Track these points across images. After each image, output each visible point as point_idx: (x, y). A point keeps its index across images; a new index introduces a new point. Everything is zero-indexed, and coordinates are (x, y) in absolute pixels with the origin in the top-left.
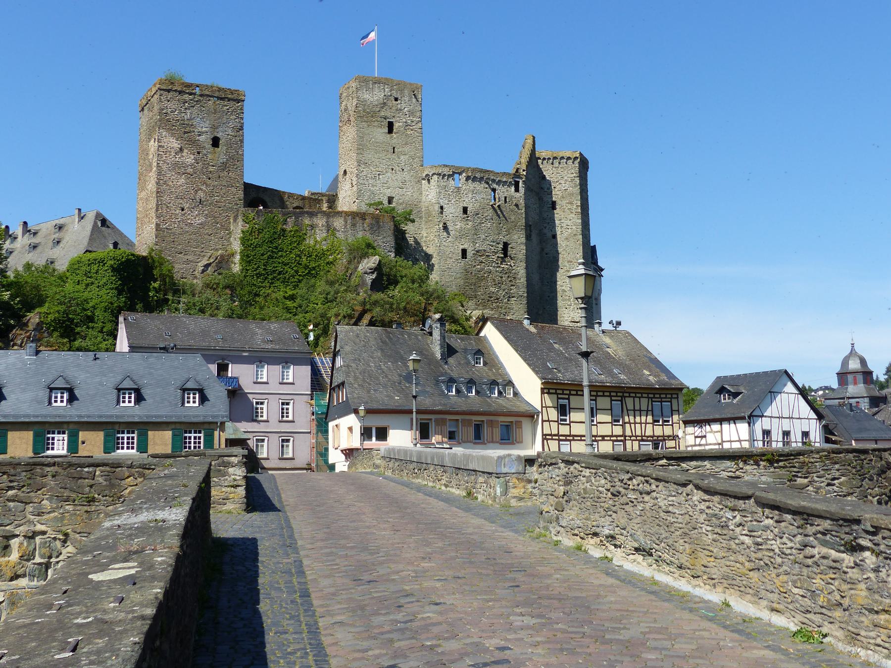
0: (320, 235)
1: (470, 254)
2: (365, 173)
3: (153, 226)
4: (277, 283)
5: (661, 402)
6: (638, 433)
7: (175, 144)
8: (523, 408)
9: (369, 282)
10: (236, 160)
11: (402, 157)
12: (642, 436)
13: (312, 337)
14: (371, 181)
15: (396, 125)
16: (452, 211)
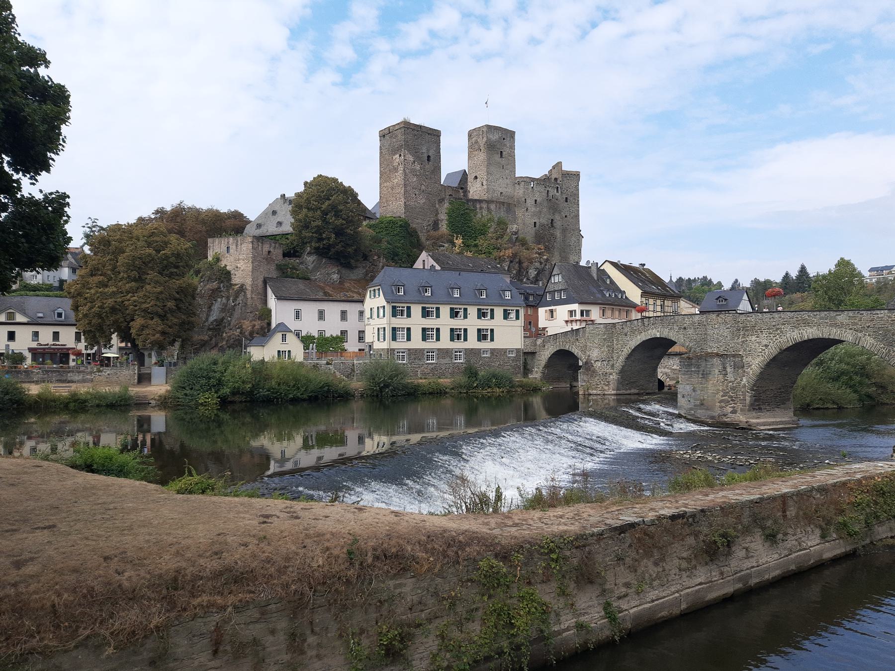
0: (485, 213)
1: (537, 225)
3: (402, 203)
7: (411, 159)
10: (437, 169)
16: (530, 202)
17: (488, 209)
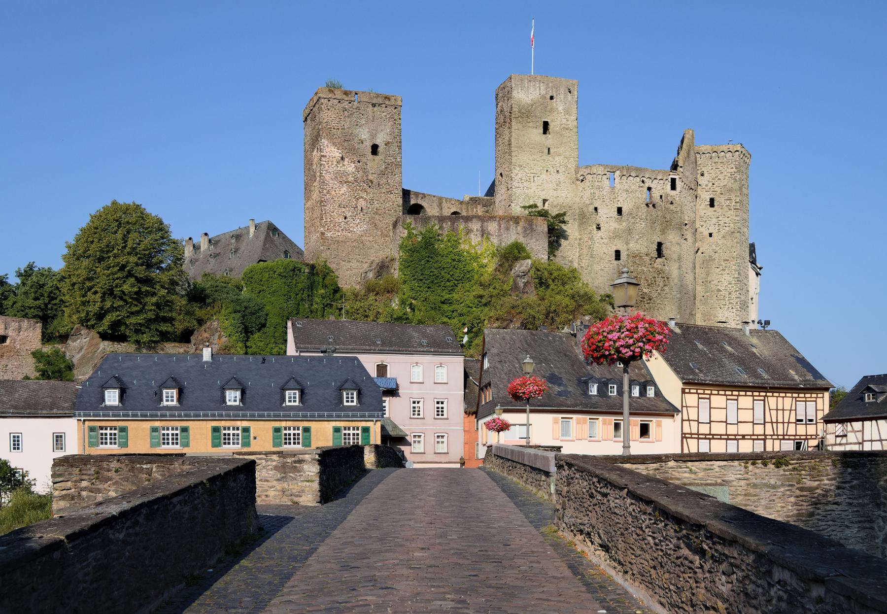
0: (475, 239)
1: (623, 255)
2: (520, 176)
4: (434, 287)
5: (806, 401)
6: (780, 432)
8: (664, 406)
9: (521, 285)
11: (557, 158)
12: (784, 435)
13: (466, 339)
14: (526, 184)
15: (551, 127)
16: (606, 214)
17: (484, 233)
